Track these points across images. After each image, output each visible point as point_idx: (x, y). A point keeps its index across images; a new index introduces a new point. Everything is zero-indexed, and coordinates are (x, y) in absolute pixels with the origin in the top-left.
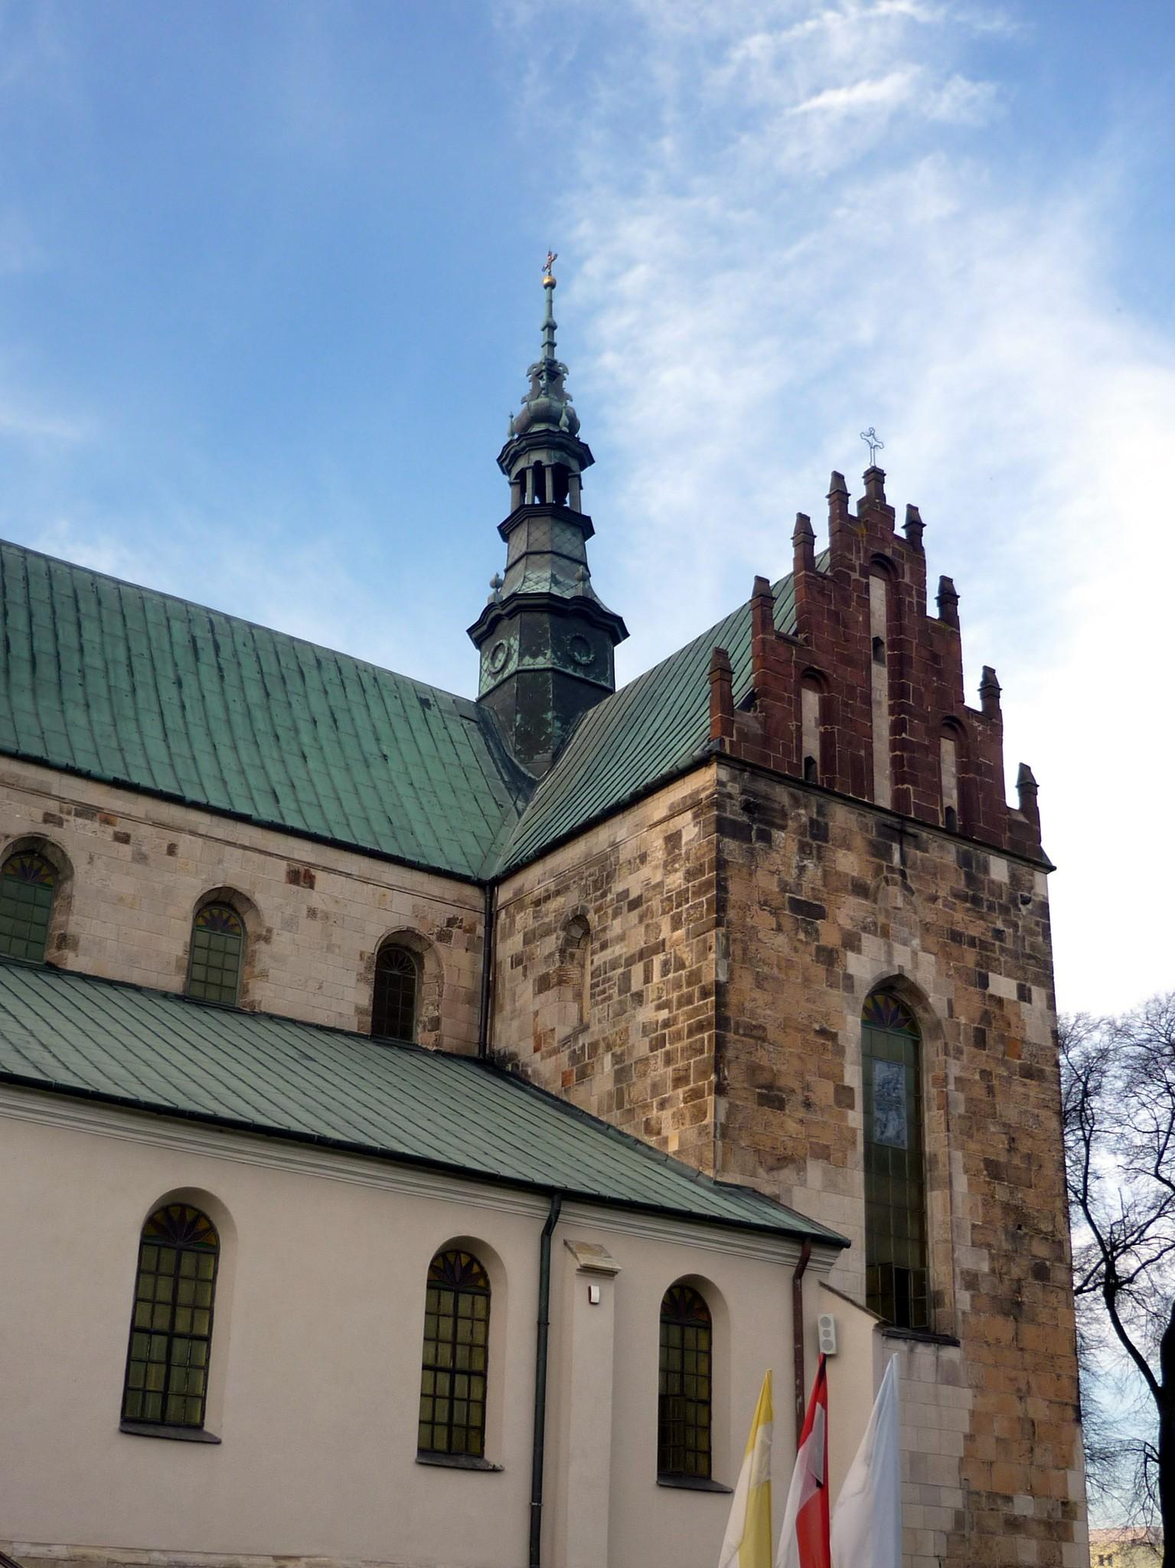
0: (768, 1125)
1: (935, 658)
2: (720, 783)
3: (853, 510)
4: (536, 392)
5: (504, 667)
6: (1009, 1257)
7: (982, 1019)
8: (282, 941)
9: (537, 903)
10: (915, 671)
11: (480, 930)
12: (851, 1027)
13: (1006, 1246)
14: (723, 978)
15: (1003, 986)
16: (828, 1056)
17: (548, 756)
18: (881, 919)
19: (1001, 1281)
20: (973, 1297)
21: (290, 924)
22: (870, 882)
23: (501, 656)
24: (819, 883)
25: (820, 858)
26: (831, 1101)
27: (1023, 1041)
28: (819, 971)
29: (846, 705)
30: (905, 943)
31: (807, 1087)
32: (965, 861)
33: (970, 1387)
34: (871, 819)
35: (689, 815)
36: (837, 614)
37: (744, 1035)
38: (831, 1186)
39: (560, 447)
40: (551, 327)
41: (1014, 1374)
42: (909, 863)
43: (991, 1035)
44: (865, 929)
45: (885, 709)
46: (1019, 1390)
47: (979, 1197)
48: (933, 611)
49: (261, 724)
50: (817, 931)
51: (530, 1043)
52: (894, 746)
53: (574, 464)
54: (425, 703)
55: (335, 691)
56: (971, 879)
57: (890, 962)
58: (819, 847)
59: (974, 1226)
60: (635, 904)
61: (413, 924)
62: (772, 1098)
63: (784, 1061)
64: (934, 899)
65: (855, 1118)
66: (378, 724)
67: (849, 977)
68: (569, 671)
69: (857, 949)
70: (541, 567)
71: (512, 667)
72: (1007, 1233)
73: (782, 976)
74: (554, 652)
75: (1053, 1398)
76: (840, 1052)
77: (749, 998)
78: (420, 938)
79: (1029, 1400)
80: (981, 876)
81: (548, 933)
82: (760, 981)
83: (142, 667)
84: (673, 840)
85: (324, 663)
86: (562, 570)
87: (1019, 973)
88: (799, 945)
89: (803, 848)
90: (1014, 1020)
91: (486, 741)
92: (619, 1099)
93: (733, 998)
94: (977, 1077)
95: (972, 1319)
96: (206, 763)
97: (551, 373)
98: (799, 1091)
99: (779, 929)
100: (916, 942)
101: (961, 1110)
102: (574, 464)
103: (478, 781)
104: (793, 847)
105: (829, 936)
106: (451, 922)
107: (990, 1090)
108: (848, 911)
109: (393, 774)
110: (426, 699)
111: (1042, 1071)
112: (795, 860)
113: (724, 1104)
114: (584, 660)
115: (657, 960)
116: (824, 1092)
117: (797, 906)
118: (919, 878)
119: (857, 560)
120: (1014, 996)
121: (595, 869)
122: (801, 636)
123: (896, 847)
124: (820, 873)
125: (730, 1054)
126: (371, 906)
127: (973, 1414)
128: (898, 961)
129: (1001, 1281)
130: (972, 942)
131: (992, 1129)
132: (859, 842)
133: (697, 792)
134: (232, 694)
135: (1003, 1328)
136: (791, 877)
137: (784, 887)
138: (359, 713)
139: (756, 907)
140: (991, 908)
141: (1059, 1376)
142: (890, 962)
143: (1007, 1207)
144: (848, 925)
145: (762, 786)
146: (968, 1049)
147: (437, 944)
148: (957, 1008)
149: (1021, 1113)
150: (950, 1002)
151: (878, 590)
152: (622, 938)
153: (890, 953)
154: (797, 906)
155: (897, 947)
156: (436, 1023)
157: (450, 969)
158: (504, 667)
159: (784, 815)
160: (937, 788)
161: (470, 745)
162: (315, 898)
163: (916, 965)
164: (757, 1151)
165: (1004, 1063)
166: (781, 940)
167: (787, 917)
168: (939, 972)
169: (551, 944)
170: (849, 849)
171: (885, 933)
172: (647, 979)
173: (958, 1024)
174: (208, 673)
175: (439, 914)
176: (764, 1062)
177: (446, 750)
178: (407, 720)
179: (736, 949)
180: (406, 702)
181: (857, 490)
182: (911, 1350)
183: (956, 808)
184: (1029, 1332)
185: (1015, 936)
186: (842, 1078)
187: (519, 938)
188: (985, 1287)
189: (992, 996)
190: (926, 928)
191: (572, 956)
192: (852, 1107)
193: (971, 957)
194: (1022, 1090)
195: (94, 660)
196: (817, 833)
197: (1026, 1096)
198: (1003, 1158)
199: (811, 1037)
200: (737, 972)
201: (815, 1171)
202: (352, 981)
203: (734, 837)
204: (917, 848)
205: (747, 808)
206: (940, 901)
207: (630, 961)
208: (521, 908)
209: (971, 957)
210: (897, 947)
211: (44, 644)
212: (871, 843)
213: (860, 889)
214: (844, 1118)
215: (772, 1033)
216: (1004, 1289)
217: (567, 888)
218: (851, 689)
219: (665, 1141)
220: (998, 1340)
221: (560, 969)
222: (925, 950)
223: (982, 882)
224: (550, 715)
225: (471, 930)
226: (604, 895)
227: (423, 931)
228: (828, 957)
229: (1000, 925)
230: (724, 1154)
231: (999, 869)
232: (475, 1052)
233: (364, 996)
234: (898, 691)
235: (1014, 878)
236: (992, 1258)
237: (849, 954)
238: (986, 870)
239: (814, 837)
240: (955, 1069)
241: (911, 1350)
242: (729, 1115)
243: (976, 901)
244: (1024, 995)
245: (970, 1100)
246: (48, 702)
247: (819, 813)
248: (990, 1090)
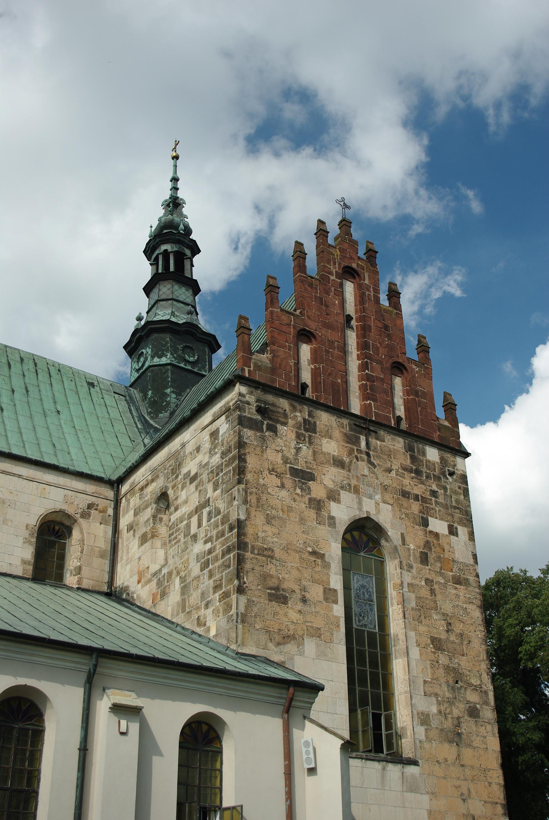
0: (275, 614)
1: (386, 327)
2: (240, 394)
5: (143, 365)
6: (451, 702)
7: (425, 546)
9: (142, 489)
10: (373, 333)
11: (110, 511)
12: (334, 550)
13: (448, 695)
14: (242, 517)
15: (438, 525)
16: (318, 569)
17: (167, 414)
18: (354, 482)
19: (446, 718)
20: (426, 730)
22: (346, 460)
23: (142, 359)
24: (310, 458)
25: (310, 443)
26: (321, 598)
27: (454, 561)
28: (311, 514)
29: (328, 352)
30: (370, 497)
31: (304, 589)
33: (428, 793)
35: (223, 417)
36: (321, 299)
37: (258, 554)
38: (321, 655)
41: (458, 783)
42: (372, 448)
43: (432, 557)
44: (342, 488)
46: (462, 794)
47: (428, 663)
48: (384, 301)
50: (309, 488)
51: (136, 578)
52: (361, 378)
54: (91, 385)
56: (413, 459)
57: (360, 509)
58: (310, 436)
59: (425, 682)
60: (193, 479)
61: (64, 507)
62: (279, 596)
64: (390, 471)
65: (339, 610)
66: (57, 394)
67: (332, 518)
68: (182, 365)
69: (337, 500)
70: (166, 308)
71: (147, 365)
72: (448, 686)
73: (285, 516)
74: (172, 354)
75: (487, 799)
76: (327, 566)
77: (259, 529)
78: (69, 516)
79: (470, 801)
80: (421, 458)
81: (146, 507)
82: (269, 520)
84: (214, 435)
85: (26, 360)
86: (179, 309)
87: (449, 518)
88: (296, 497)
89: (299, 436)
90: (446, 548)
91: (129, 406)
92: (183, 605)
93: (250, 530)
94: (423, 583)
95: (427, 745)
97: (174, 204)
98: (298, 591)
99: (283, 486)
100: (378, 497)
101: (413, 604)
103: (119, 427)
104: (293, 436)
105: (318, 491)
106: (90, 506)
107: (433, 592)
108: (330, 476)
109: (62, 422)
111: (467, 580)
112: (293, 444)
113: (243, 600)
114: (191, 359)
116: (316, 592)
117: (295, 472)
118: (379, 457)
119: (335, 269)
120: (446, 532)
121: (172, 462)
122: (298, 312)
123: (363, 438)
124: (311, 452)
125: (248, 566)
127: (430, 812)
128: (365, 509)
129: (446, 718)
130: (416, 498)
131: (435, 617)
132: (337, 434)
133: (228, 403)
135: (448, 751)
136: (290, 453)
137: (286, 461)
139: (266, 472)
140: (427, 477)
141: (490, 784)
142: (360, 509)
143: (447, 669)
144: (331, 485)
145: (270, 398)
146: (416, 565)
147: (81, 520)
148: (407, 539)
149: (454, 606)
150: (402, 535)
152: (186, 502)
153: (360, 503)
154: (295, 472)
155: (365, 500)
156: (79, 570)
158: (143, 365)
159: (286, 416)
160: (392, 404)
161: (118, 408)
163: (378, 512)
164: (268, 631)
165: (442, 575)
166: (284, 493)
167: (288, 481)
168: (394, 515)
169: (148, 513)
170: (331, 438)
171: (356, 491)
172: (200, 525)
173: (409, 549)
175: (83, 501)
176: (273, 572)
177: (101, 411)
178: (77, 393)
179: (252, 499)
180: (78, 384)
181: (333, 229)
182: (384, 769)
183: (403, 417)
184: (467, 753)
185: (445, 494)
186: (328, 583)
187: (132, 513)
188: (435, 723)
189: (431, 532)
190: (385, 488)
191: (161, 520)
192: (336, 602)
193: (415, 507)
194: (454, 592)
196: (309, 427)
197: (457, 596)
198: (443, 636)
199: (306, 556)
200: (253, 513)
201: (310, 646)
202: (20, 543)
203: (251, 428)
204: (377, 439)
205: (259, 410)
206: (394, 472)
207: (190, 516)
208: (134, 494)
209: (415, 507)
210: (365, 500)
212: (345, 434)
213: (339, 463)
214: (331, 610)
215: (278, 553)
216: (448, 724)
217: (158, 477)
218: (331, 343)
219: (208, 630)
220: (446, 760)
221: (153, 528)
222: (384, 502)
223: (422, 461)
224: (168, 391)
225: (104, 511)
226: (177, 477)
227: (70, 511)
228: (317, 505)
229: (434, 488)
230: (244, 633)
231: (432, 454)
232: (105, 589)
234: (363, 346)
235: (442, 459)
236: (439, 703)
237: (332, 503)
238: (424, 454)
239: (306, 430)
240: (408, 578)
241: (384, 769)
242: (247, 607)
243: (418, 472)
244: (453, 531)
245: (418, 598)
247: (310, 415)
248: (433, 592)
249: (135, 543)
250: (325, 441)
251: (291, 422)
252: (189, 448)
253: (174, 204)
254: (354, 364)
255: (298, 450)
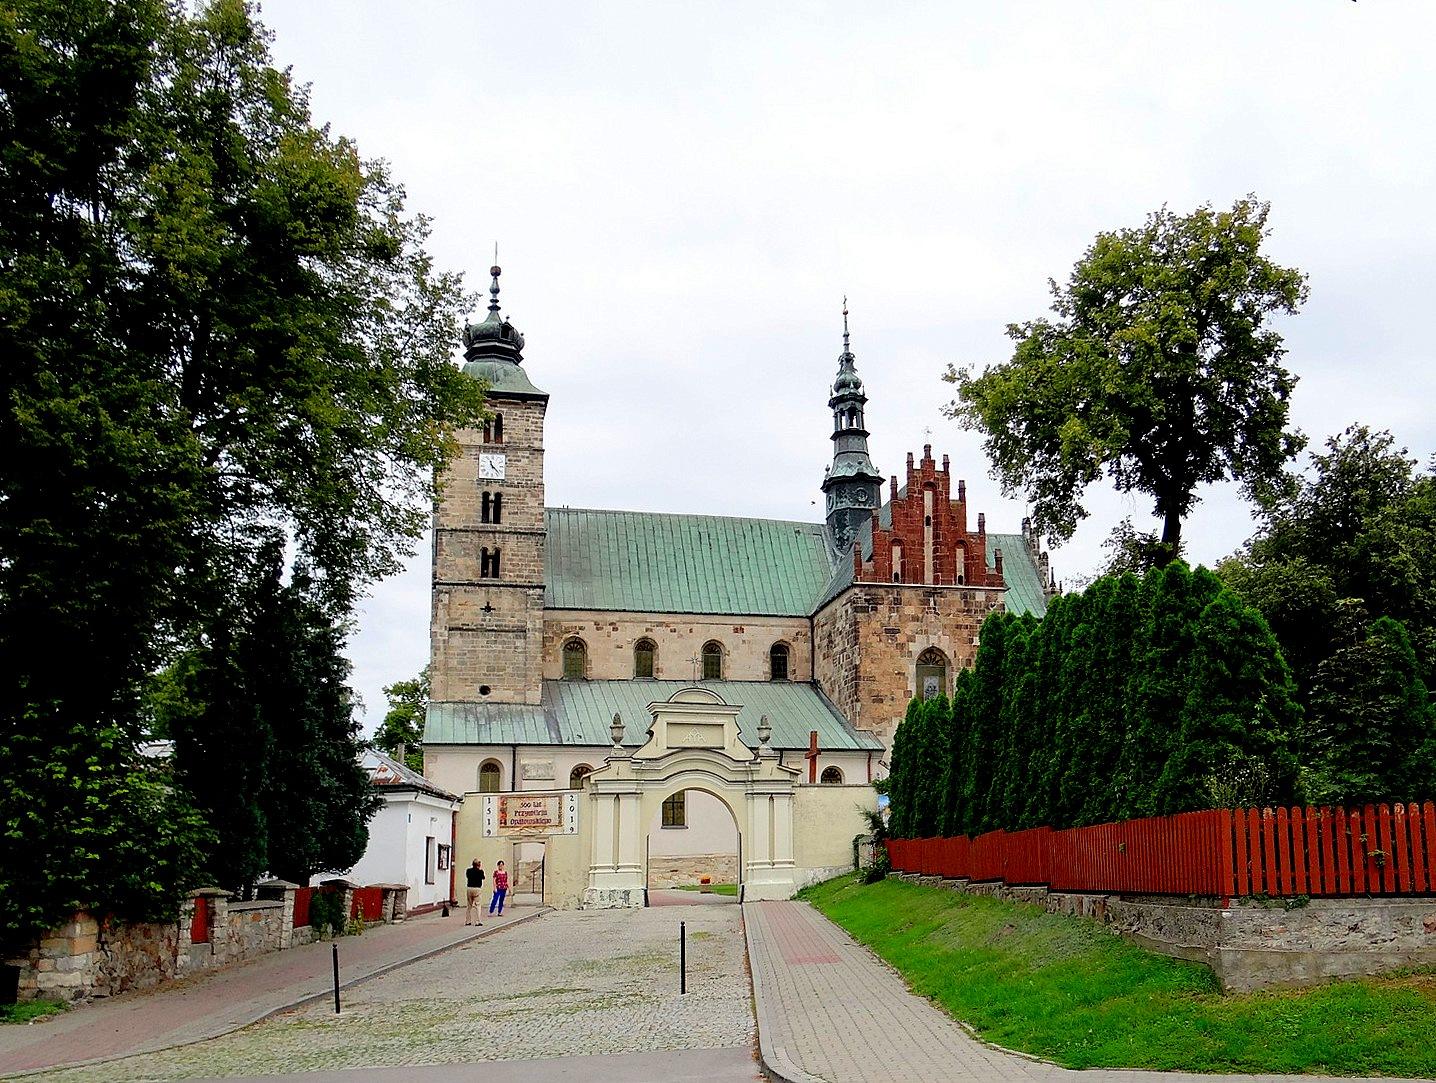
3: (917, 465)
4: (841, 372)
8: (734, 655)
11: (809, 634)
12: (911, 669)
14: (858, 663)
18: (924, 628)
21: (736, 647)
22: (920, 615)
24: (897, 621)
25: (898, 611)
29: (910, 549)
32: (965, 596)
34: (920, 592)
39: (851, 399)
40: (846, 336)
45: (931, 544)
49: (726, 567)
53: (858, 405)
55: (758, 540)
57: (928, 642)
63: (882, 687)
68: (857, 507)
71: (834, 508)
77: (868, 667)
83: (679, 554)
84: (847, 611)
85: (754, 527)
89: (891, 610)
93: (862, 669)
96: (703, 592)
97: (848, 360)
102: (858, 405)
106: (797, 634)
108: (910, 628)
110: (798, 529)
113: (859, 704)
115: (845, 653)
123: (932, 599)
126: (765, 636)
132: (915, 601)
134: (715, 555)
137: (882, 625)
138: (767, 547)
142: (928, 642)
145: (873, 591)
151: (928, 496)
157: (799, 650)
160: (955, 571)
162: (744, 636)
167: (884, 636)
171: (926, 632)
174: (705, 548)
195: (661, 557)
196: (898, 601)
211: (643, 557)
213: (915, 619)
228: (901, 646)
233: (767, 667)
234: (936, 536)
237: (910, 644)
246: (645, 582)
249: (821, 657)
250: (906, 608)
251: (886, 602)
252: (838, 615)
253: (848, 360)
254: (928, 550)
255: (890, 617)
